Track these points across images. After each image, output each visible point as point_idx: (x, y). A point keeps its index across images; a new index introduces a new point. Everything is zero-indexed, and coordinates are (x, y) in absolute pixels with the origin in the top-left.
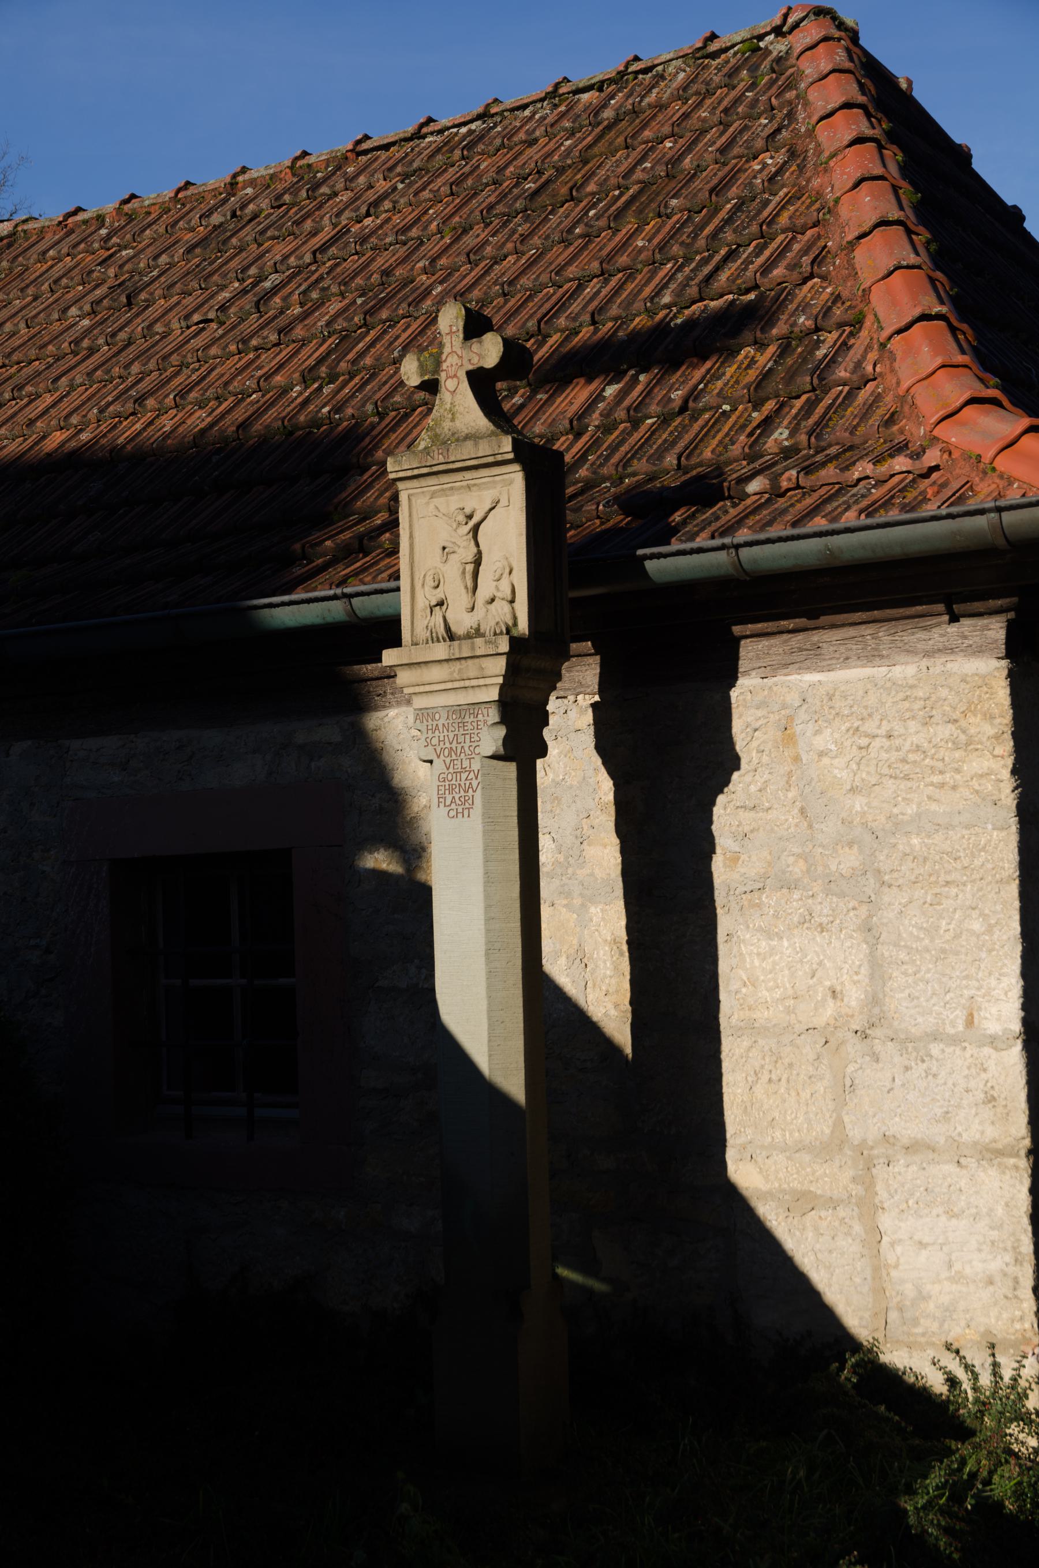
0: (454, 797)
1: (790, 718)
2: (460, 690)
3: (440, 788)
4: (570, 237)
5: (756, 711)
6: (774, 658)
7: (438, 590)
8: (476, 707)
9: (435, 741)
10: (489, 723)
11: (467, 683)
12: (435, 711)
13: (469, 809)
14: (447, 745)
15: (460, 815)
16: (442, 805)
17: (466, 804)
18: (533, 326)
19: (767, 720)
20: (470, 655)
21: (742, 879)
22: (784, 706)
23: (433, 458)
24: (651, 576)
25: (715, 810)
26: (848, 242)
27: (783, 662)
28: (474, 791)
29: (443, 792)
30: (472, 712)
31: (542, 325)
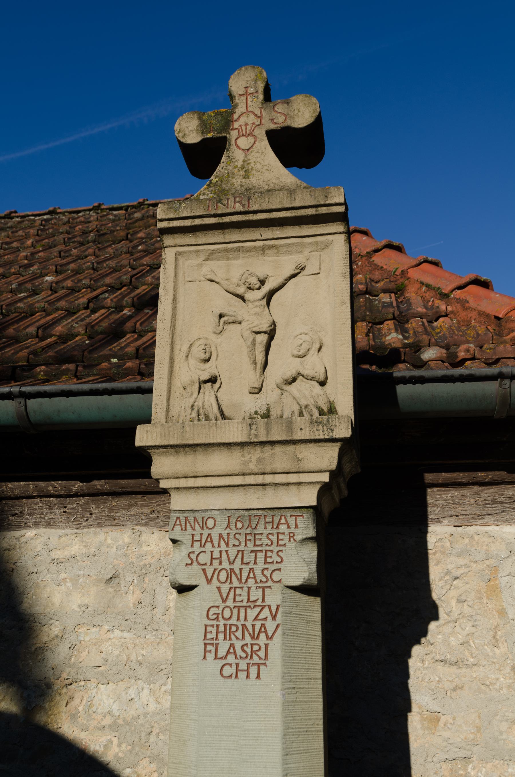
0: (232, 645)
1: (495, 569)
2: (252, 489)
3: (209, 629)
4: (134, 251)
5: (457, 559)
6: (466, 507)
7: (209, 364)
8: (278, 513)
9: (204, 558)
10: (299, 537)
11: (268, 479)
12: (207, 515)
13: (259, 665)
14: (226, 565)
15: (242, 675)
16: (210, 656)
17: (255, 657)
18: (126, 279)
19: (469, 569)
20: (284, 438)
21: (445, 744)
22: (489, 557)
23: (227, 206)
24: (400, 401)
25: (411, 662)
26: (367, 253)
27: (478, 512)
28: (269, 638)
29: (214, 635)
30: (269, 519)
31: (133, 279)
